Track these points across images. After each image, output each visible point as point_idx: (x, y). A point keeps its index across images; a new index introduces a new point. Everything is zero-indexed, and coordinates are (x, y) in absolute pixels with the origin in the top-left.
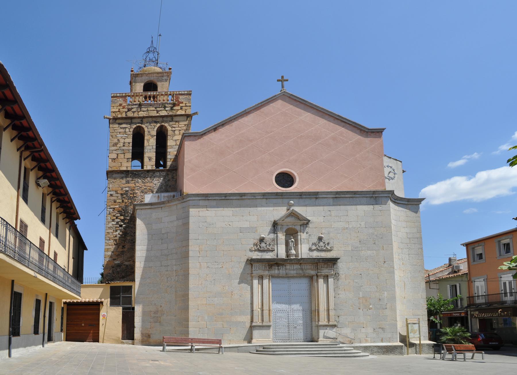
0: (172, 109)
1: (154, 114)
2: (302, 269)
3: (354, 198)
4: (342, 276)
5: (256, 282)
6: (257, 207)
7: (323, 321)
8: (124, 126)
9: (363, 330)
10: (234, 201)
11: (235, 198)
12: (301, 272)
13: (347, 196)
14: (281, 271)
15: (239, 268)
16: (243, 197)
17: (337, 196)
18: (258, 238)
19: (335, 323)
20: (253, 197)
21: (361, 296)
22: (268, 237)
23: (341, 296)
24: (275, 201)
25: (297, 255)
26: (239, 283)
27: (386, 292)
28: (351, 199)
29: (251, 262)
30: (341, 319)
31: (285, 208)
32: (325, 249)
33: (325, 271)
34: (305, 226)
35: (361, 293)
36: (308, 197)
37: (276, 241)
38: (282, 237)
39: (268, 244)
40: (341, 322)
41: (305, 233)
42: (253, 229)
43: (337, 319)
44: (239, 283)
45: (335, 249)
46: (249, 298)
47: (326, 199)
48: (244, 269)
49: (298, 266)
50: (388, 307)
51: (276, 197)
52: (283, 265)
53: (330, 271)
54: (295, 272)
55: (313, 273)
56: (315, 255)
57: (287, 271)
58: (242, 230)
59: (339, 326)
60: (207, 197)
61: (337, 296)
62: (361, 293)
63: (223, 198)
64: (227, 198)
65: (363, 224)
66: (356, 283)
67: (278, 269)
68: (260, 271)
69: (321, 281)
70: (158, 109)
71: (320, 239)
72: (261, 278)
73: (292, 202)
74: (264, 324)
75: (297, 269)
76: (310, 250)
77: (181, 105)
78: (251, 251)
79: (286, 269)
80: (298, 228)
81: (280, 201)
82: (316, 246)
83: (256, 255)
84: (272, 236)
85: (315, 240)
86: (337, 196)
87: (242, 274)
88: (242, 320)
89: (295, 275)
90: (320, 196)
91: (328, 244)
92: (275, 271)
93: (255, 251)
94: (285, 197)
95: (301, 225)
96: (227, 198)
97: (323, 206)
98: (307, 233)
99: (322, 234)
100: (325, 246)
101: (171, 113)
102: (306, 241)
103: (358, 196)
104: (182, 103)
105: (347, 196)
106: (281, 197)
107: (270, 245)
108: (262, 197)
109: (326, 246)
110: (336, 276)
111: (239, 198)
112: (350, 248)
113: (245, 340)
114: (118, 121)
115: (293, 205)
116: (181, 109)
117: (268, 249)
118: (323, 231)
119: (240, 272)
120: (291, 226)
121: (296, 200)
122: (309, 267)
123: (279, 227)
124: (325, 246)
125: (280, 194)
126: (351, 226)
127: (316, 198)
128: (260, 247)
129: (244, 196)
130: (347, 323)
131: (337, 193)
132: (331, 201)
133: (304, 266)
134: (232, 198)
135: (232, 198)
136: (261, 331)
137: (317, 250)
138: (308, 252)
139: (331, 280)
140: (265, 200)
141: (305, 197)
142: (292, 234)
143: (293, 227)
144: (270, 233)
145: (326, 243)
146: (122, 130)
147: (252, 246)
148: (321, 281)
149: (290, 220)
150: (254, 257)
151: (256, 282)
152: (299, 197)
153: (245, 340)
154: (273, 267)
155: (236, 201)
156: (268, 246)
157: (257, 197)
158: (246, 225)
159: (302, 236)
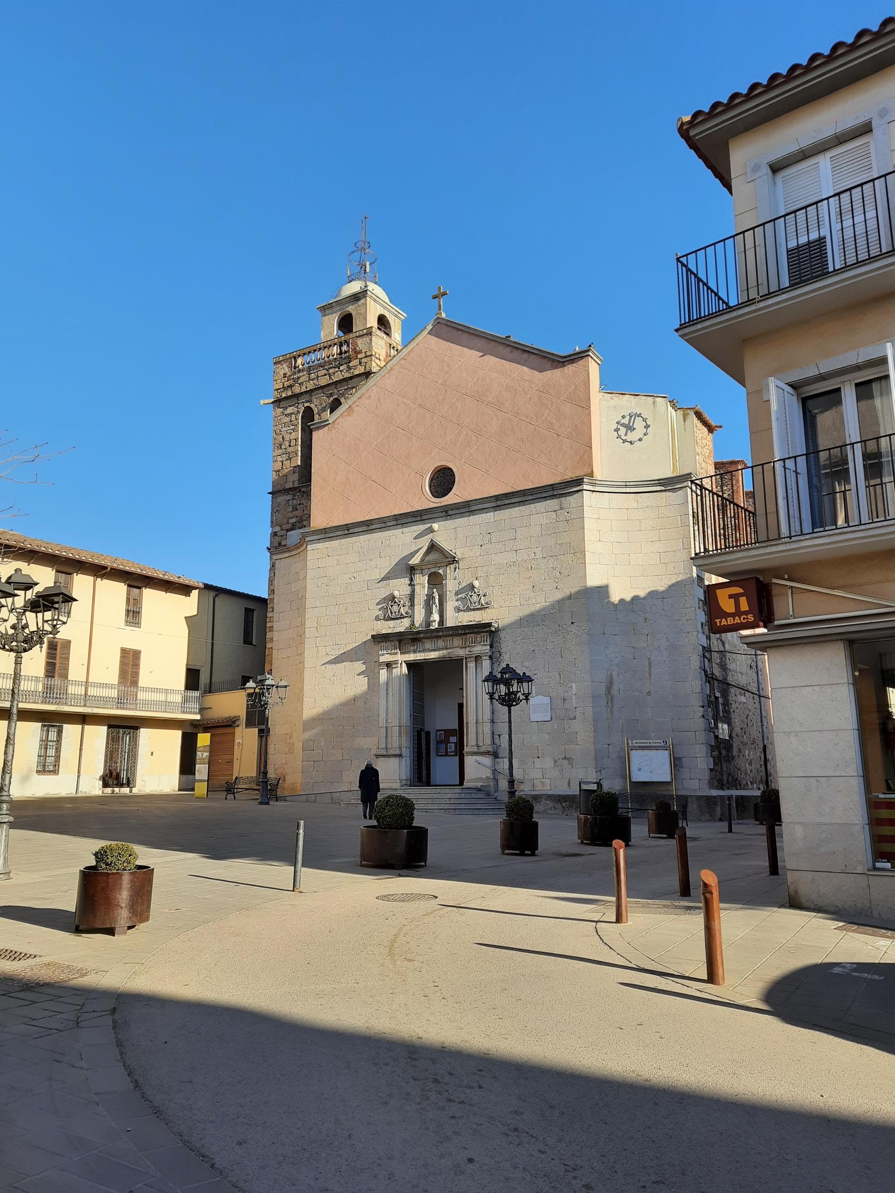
0: (349, 368)
1: (324, 381)
8: (290, 410)
9: (538, 763)
13: (513, 501)
16: (371, 527)
17: (499, 503)
20: (383, 525)
27: (574, 684)
36: (458, 511)
50: (578, 714)
60: (326, 533)
63: (346, 532)
64: (351, 531)
65: (538, 551)
70: (331, 371)
77: (359, 356)
86: (499, 503)
96: (351, 531)
101: (347, 375)
103: (530, 497)
104: (360, 352)
105: (513, 501)
108: (395, 523)
111: (365, 528)
114: (283, 404)
116: (360, 363)
131: (497, 498)
134: (356, 530)
135: (356, 530)
141: (450, 512)
146: (287, 419)
157: (389, 524)
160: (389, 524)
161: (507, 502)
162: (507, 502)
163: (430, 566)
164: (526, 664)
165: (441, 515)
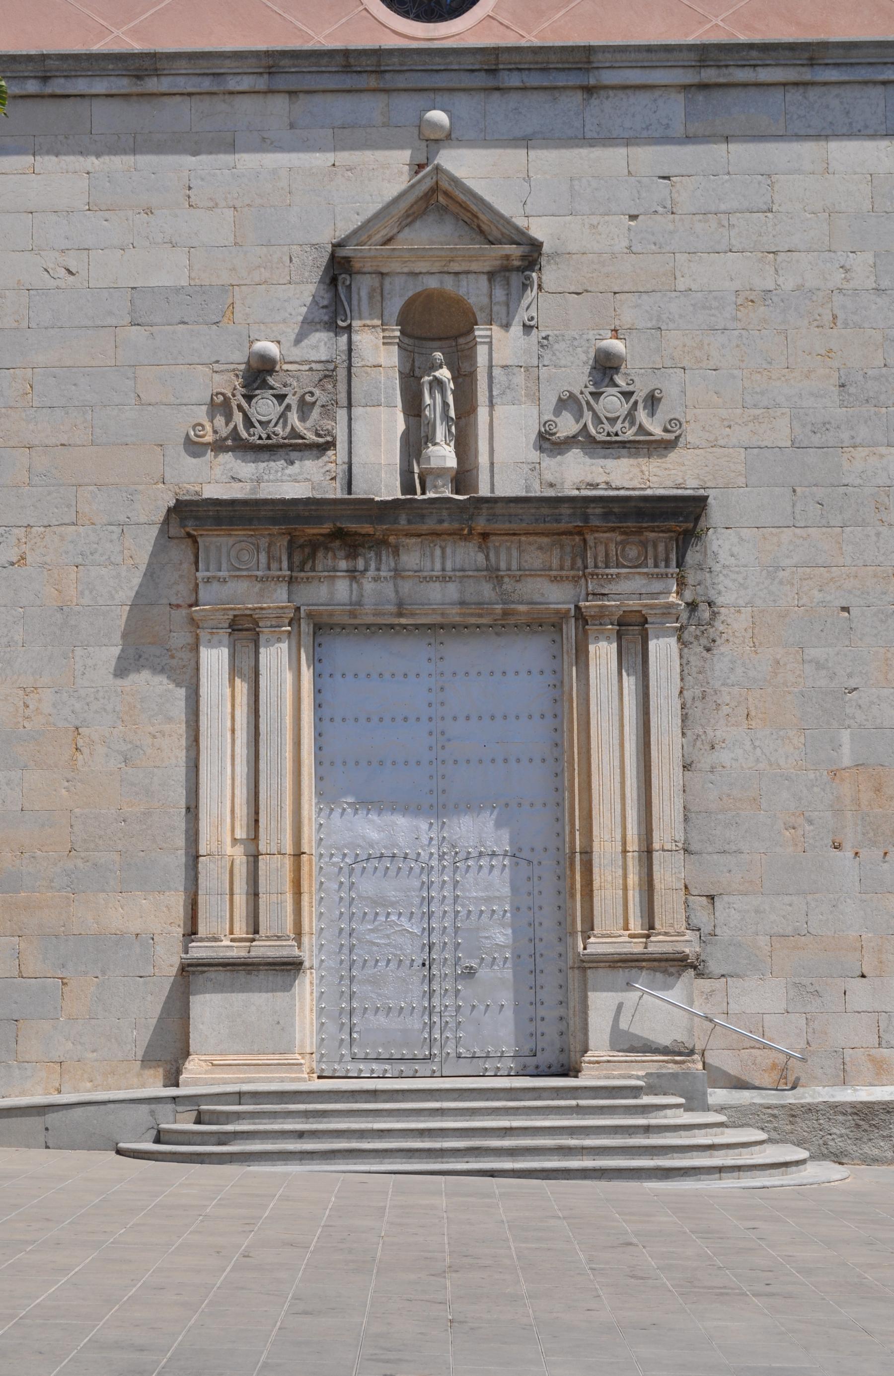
2: (494, 575)
3: (813, 94)
4: (734, 623)
5: (214, 660)
6: (232, 147)
7: (612, 936)
10: (98, 106)
11: (100, 86)
12: (487, 591)
13: (764, 75)
14: (368, 586)
15: (120, 563)
16: (152, 85)
17: (710, 75)
18: (239, 357)
19: (689, 945)
20: (206, 84)
21: (846, 761)
22: (296, 353)
23: (724, 756)
24: (341, 107)
25: (463, 478)
26: (121, 670)
28: (794, 95)
29: (191, 520)
30: (731, 916)
31: (400, 158)
32: (630, 434)
33: (629, 589)
34: (516, 279)
35: (845, 736)
36: (535, 80)
37: (339, 375)
38: (377, 351)
39: (292, 400)
40: (724, 933)
41: (516, 329)
42: (208, 303)
43: (702, 918)
44: (121, 670)
45: (692, 434)
46: (180, 773)
47: (643, 98)
48: (151, 575)
49: (465, 555)
51: (349, 81)
52: (380, 544)
53: (657, 586)
54: (452, 591)
55: (557, 596)
56: (575, 473)
57: (406, 587)
58: (142, 307)
59: (713, 967)
61: (705, 760)
62: (845, 736)
63: (32, 87)
65: (862, 262)
66: (819, 665)
67: (353, 575)
68: (242, 587)
69: (603, 653)
71: (606, 367)
72: (245, 631)
73: (438, 116)
74: (263, 949)
75: (462, 575)
76: (548, 442)
78: (194, 447)
79: (398, 573)
80: (475, 292)
81: (371, 107)
82: (579, 416)
83: (225, 479)
84: (321, 346)
85: (576, 376)
86: (710, 75)
87: (140, 605)
88: (135, 926)
89: (454, 614)
90: (609, 77)
91: (653, 401)
92: (334, 589)
93: (219, 447)
94: (401, 81)
95: (491, 275)
96: (57, 86)
97: (628, 142)
98: (527, 328)
99: (615, 333)
100: (631, 417)
102: (520, 378)
103: (832, 75)
105: (764, 75)
106: (372, 82)
107: (305, 408)
108: (261, 83)
109: (642, 416)
110: (697, 620)
111: (123, 85)
112: (780, 432)
113: (148, 1061)
115: (447, 138)
117: (295, 434)
118: (627, 317)
119: (127, 594)
120: (432, 283)
121: (465, 104)
122: (534, 558)
123: (363, 286)
124: (631, 417)
125: (368, 63)
126: (788, 283)
127: (589, 90)
128: (249, 423)
129: (157, 73)
130: (763, 941)
131: (706, 54)
132: (674, 107)
133: (506, 556)
134: (81, 86)
135: (81, 86)
136: (237, 999)
137: (587, 442)
138: (535, 455)
139: (662, 650)
140: (279, 103)
141: (514, 80)
142: (437, 332)
143: (449, 284)
144: (308, 325)
145: (640, 396)
147: (201, 414)
148: (603, 653)
149: (430, 236)
150: (211, 492)
151: (214, 660)
152: (481, 80)
153: (148, 1061)
154: (323, 561)
155: (115, 106)
156: (294, 418)
157: (232, 84)
158: (170, 271)
159: (500, 346)
160: (232, 84)
161: (742, 75)
162: (742, 75)
163: (421, 266)
164: (812, 653)
165: (467, 81)
